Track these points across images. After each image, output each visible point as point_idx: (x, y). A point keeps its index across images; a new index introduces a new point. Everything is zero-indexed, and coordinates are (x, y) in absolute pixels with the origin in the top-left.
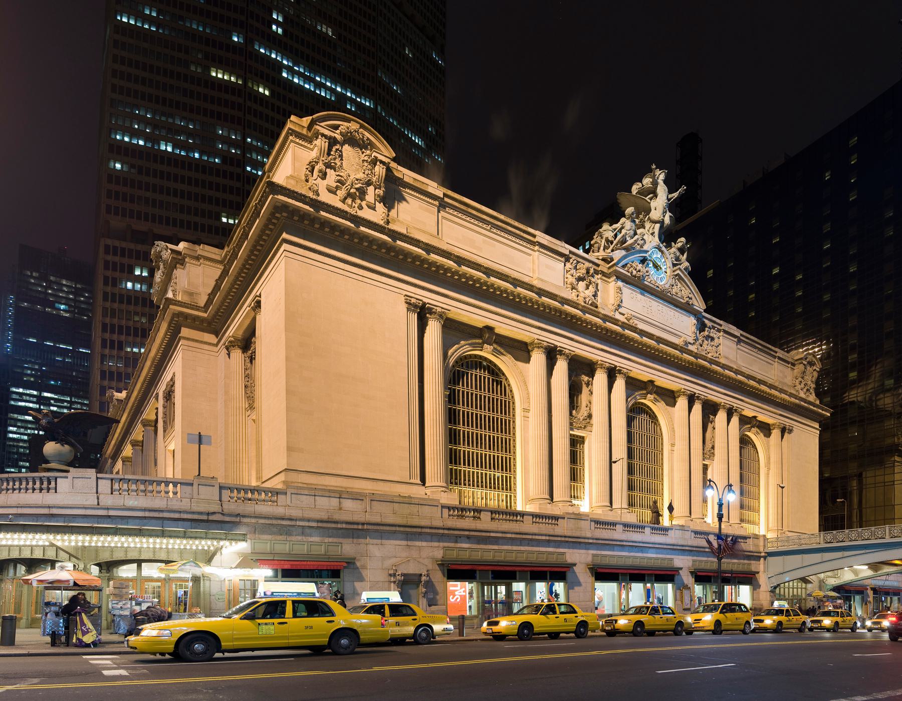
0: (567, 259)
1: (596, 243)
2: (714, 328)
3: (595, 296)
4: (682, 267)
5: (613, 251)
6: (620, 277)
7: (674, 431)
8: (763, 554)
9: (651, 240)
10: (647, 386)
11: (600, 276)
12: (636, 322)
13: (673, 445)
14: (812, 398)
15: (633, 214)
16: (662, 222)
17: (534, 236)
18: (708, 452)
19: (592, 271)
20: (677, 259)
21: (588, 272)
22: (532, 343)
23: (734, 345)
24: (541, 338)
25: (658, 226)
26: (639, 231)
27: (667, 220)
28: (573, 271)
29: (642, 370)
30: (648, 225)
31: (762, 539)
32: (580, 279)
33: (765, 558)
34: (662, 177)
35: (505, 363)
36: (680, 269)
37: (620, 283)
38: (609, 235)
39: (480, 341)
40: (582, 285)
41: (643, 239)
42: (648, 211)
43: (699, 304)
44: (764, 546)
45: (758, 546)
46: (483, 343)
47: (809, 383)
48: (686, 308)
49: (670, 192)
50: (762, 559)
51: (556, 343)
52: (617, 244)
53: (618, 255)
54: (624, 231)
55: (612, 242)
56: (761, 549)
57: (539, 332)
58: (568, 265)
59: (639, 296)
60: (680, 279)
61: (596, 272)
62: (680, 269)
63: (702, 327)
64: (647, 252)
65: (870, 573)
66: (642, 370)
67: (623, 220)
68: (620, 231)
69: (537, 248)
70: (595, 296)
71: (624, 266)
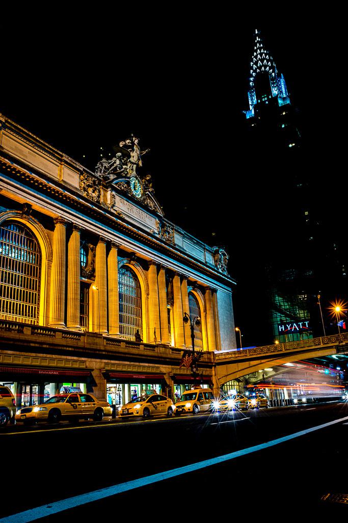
0: (82, 173)
1: (99, 168)
2: (169, 227)
3: (99, 197)
4: (150, 190)
5: (109, 174)
6: (113, 189)
7: (148, 286)
8: (214, 364)
9: (131, 170)
10: (131, 256)
11: (101, 187)
12: (124, 216)
13: (148, 294)
14: (226, 273)
15: (121, 156)
16: (138, 165)
17: (62, 156)
18: (170, 299)
19: (97, 183)
20: (147, 185)
21: (94, 182)
22: (56, 219)
23: (181, 239)
24: (63, 216)
25: (135, 166)
26: (124, 167)
27: (141, 164)
28: (85, 181)
29: (128, 245)
30: (129, 165)
31: (212, 355)
32: (89, 186)
33: (215, 366)
34: (136, 142)
35: (37, 229)
36: (149, 191)
37: (114, 193)
38: (107, 165)
39: (21, 212)
40: (90, 190)
41: (127, 171)
42: (129, 156)
43: (160, 213)
44: (214, 359)
45: (210, 359)
46: (23, 213)
47: (224, 265)
48: (154, 213)
49: (141, 150)
50: (213, 368)
51: (73, 221)
52: (111, 171)
53: (112, 177)
54: (115, 165)
55: (108, 170)
56: (213, 361)
57: (62, 212)
58: (82, 177)
59: (126, 202)
60: (149, 196)
61: (99, 184)
62: (149, 191)
63: (163, 226)
64: (129, 178)
65: (274, 373)
66: (128, 245)
67: (114, 159)
68: (113, 165)
69: (63, 163)
70: (99, 197)
71: (116, 184)
